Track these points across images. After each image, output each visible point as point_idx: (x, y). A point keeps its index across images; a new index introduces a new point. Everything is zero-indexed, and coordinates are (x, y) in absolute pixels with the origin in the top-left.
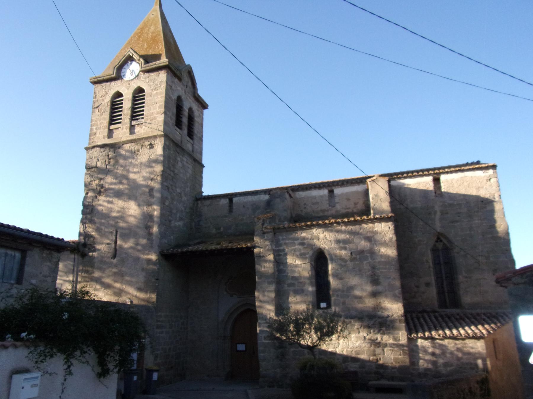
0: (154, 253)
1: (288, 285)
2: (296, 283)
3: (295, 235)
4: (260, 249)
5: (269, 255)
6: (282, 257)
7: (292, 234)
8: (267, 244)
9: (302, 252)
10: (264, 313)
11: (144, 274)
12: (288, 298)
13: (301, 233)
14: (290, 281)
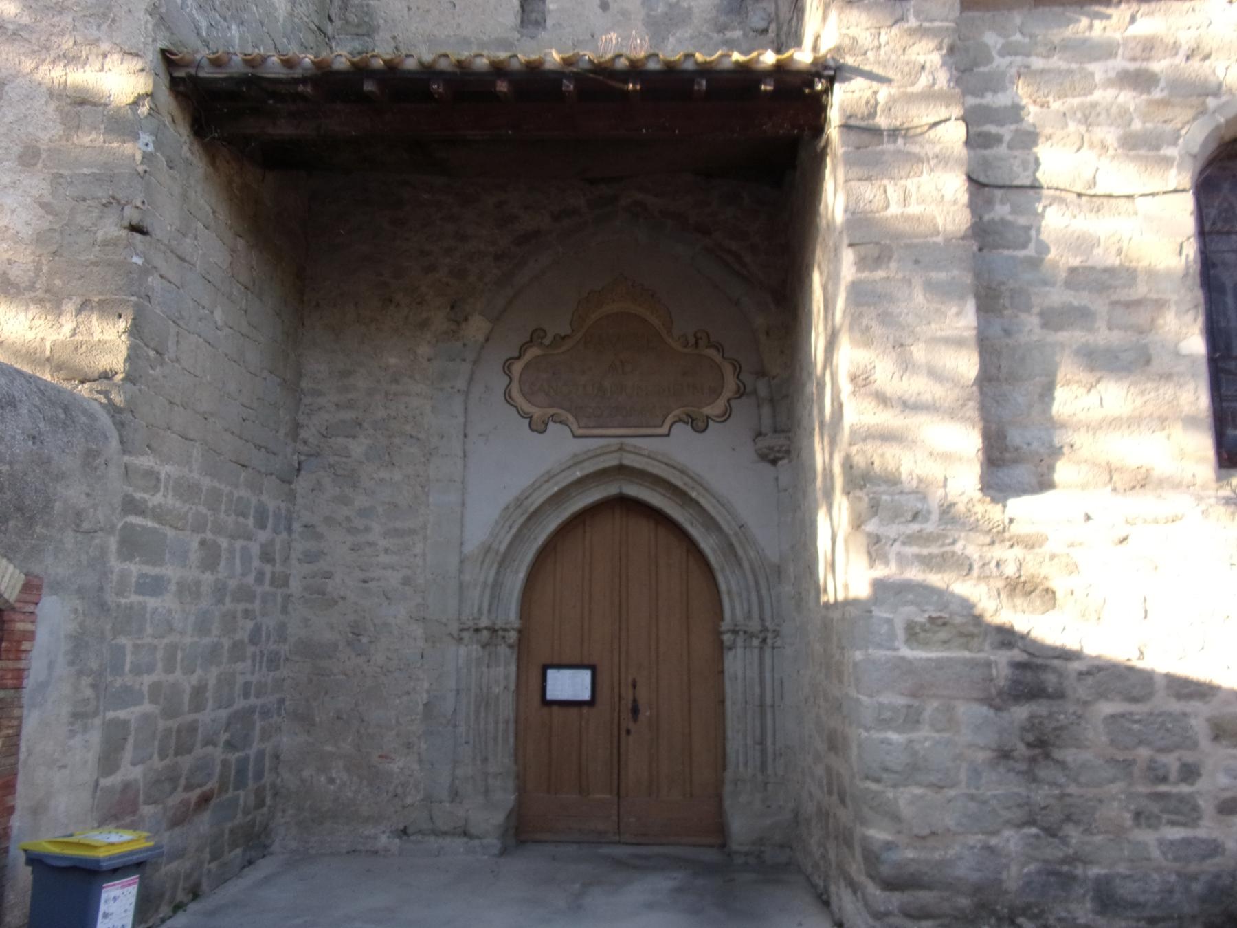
0: (116, 57)
1: (1041, 314)
2: (1099, 305)
3: (1091, 27)
4: (875, 85)
5: (936, 124)
6: (1002, 150)
7: (1070, 21)
8: (921, 59)
9: (1137, 125)
10: (904, 477)
11: (37, 184)
12: (1047, 392)
13: (1128, 19)
14: (1057, 297)
